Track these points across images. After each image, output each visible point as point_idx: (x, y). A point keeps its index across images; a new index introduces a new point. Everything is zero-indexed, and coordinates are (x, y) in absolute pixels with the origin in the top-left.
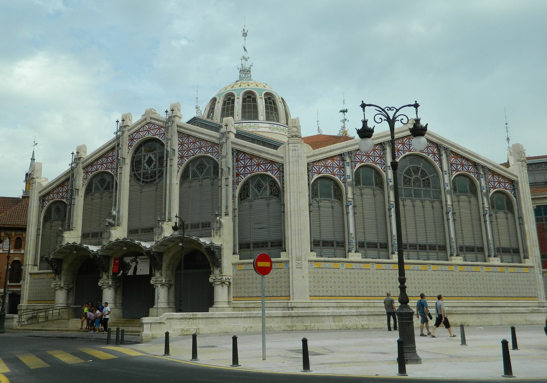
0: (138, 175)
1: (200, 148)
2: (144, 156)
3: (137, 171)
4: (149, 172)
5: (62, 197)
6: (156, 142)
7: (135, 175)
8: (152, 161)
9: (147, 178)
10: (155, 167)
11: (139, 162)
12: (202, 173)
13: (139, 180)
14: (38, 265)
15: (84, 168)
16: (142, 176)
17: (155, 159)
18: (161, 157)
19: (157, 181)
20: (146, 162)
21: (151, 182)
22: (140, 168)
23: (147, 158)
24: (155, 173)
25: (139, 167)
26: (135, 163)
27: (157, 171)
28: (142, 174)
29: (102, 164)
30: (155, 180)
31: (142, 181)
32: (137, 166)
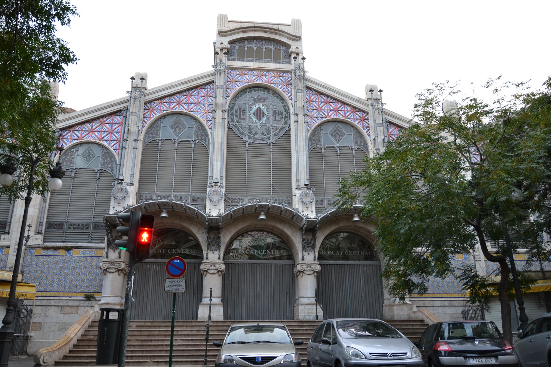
0: (241, 127)
3: (238, 122)
4: (259, 127)
5: (102, 139)
6: (268, 92)
7: (235, 126)
9: (256, 133)
11: (243, 112)
12: (339, 141)
13: (243, 133)
14: (43, 234)
15: (145, 104)
16: (247, 130)
18: (277, 112)
20: (254, 114)
22: (245, 119)
23: (254, 108)
24: (268, 130)
25: (242, 117)
26: (236, 111)
27: (271, 127)
28: (247, 126)
30: (269, 138)
31: (247, 136)
32: (239, 116)
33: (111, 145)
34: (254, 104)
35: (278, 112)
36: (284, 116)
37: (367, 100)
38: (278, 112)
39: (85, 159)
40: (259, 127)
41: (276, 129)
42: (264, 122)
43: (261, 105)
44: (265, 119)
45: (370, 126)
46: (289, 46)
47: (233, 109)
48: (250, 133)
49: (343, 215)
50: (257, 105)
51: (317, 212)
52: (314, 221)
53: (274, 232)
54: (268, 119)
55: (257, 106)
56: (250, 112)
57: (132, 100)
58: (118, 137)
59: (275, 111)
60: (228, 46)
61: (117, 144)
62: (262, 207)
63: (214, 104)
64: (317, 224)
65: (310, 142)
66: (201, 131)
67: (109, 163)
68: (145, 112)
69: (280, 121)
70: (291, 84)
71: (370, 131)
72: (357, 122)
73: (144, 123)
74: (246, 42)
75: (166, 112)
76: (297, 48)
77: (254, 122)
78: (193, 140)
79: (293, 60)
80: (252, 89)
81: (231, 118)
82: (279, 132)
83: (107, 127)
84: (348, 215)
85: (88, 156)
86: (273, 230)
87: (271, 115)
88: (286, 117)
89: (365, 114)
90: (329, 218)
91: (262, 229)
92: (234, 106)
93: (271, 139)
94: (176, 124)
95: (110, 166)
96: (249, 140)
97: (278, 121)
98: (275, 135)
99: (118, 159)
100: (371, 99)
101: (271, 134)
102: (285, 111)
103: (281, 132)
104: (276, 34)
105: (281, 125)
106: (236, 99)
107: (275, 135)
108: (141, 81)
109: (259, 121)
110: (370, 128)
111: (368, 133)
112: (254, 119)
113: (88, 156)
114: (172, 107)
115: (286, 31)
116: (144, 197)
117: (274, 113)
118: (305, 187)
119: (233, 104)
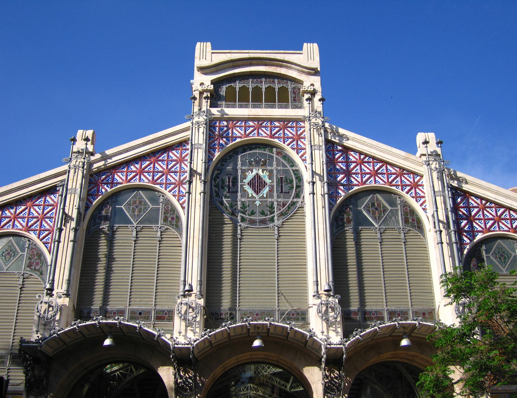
1: (376, 173)
2: (243, 172)
4: (258, 203)
8: (265, 184)
9: (253, 213)
10: (270, 194)
17: (270, 181)
19: (276, 222)
20: (250, 184)
21: (263, 222)
23: (250, 176)
24: (272, 207)
29: (142, 172)
30: (272, 220)
33: (41, 237)
34: (249, 170)
35: (286, 179)
36: (295, 186)
37: (420, 157)
38: (286, 179)
39: (3, 258)
40: (258, 203)
41: (284, 205)
42: (265, 196)
43: (261, 170)
44: (266, 190)
45: (426, 195)
46: (301, 82)
47: (218, 178)
48: (244, 213)
49: (386, 337)
50: (254, 170)
51: (346, 334)
52: (338, 348)
53: (279, 364)
54: (271, 191)
55: (255, 172)
56: (244, 181)
57: (72, 171)
58: (52, 224)
59: (282, 178)
60: (212, 87)
61: (50, 236)
62: (258, 328)
63: (188, 172)
64: (343, 354)
65: (335, 223)
66: (171, 213)
67: (37, 264)
68: (90, 187)
69: (289, 192)
70: (304, 138)
71: (427, 203)
72: (406, 190)
73: (88, 203)
74: (237, 82)
75: (120, 186)
76: (312, 85)
77: (250, 196)
78: (160, 225)
79: (306, 103)
80: (246, 148)
81: (216, 191)
82: (288, 210)
83: (37, 211)
84: (395, 336)
85: (8, 254)
86: (278, 362)
87: (275, 184)
88: (298, 187)
89: (418, 178)
90: (362, 343)
91: (263, 360)
92: (219, 174)
93: (276, 221)
94: (135, 202)
95: (37, 268)
96: (242, 224)
97: (285, 193)
98: (282, 214)
99: (49, 258)
100: (425, 155)
101: (276, 213)
102: (296, 178)
103: (291, 210)
104: (281, 66)
105: (291, 200)
106: (223, 163)
107: (282, 214)
108: (85, 142)
109: (257, 194)
110: (427, 198)
111: (423, 207)
112: (250, 191)
113: (8, 254)
114: (129, 178)
115: (295, 62)
116: (86, 314)
117: (280, 181)
118: (326, 295)
119: (218, 170)
